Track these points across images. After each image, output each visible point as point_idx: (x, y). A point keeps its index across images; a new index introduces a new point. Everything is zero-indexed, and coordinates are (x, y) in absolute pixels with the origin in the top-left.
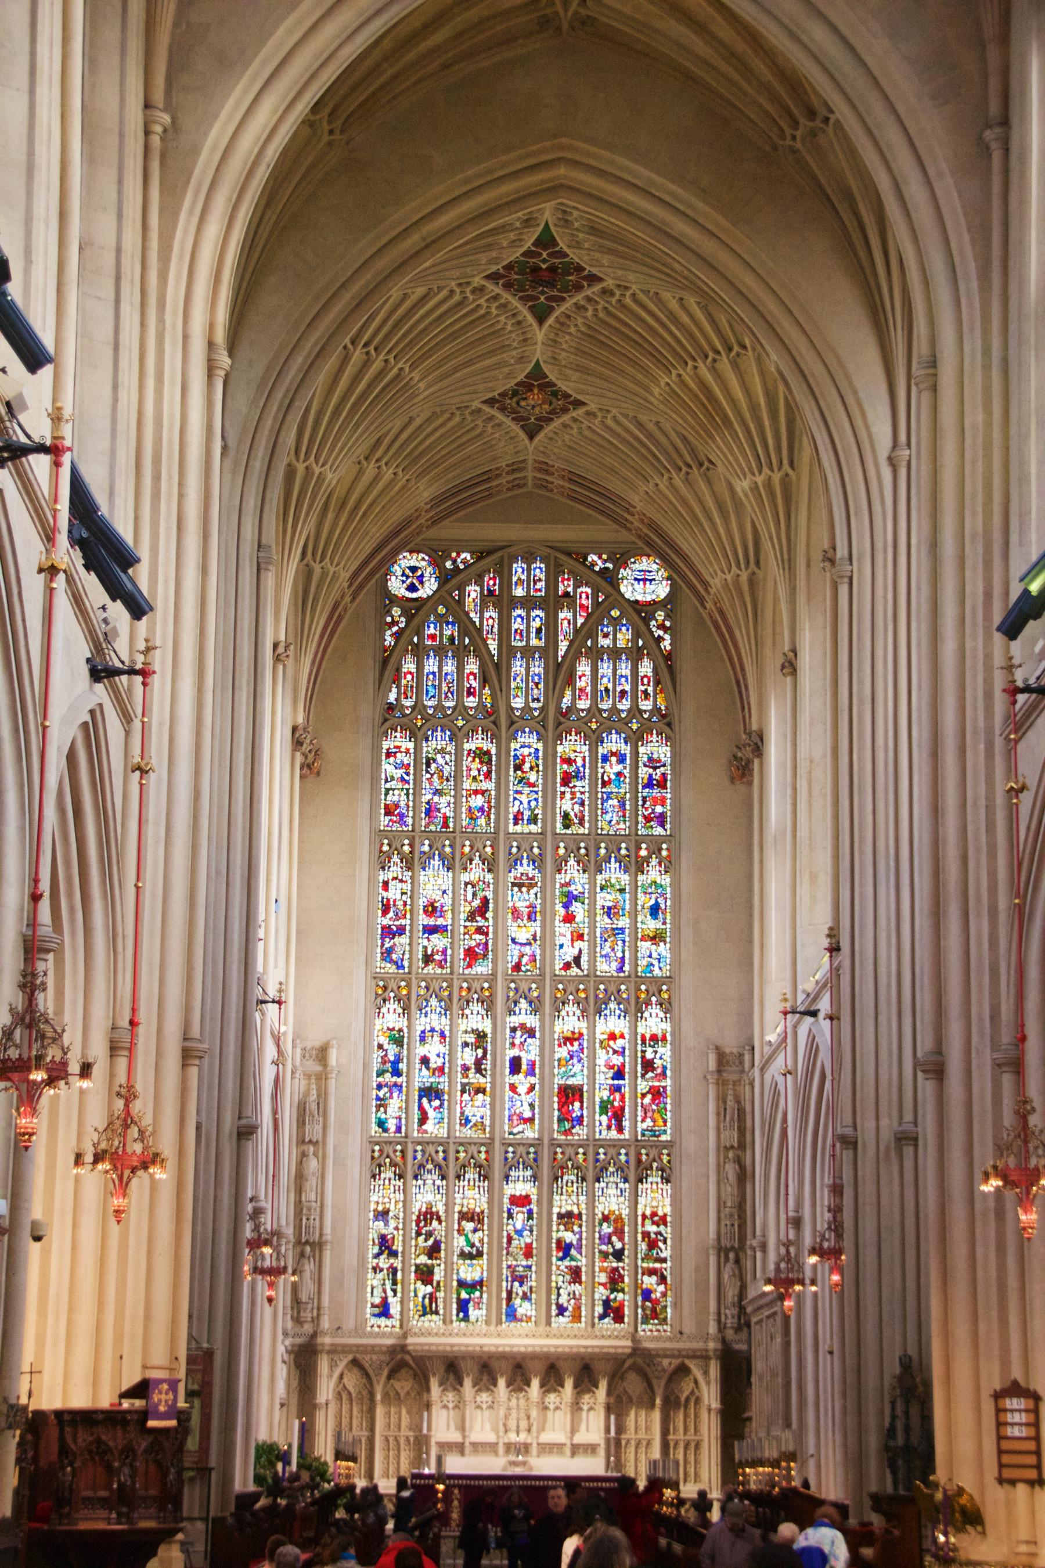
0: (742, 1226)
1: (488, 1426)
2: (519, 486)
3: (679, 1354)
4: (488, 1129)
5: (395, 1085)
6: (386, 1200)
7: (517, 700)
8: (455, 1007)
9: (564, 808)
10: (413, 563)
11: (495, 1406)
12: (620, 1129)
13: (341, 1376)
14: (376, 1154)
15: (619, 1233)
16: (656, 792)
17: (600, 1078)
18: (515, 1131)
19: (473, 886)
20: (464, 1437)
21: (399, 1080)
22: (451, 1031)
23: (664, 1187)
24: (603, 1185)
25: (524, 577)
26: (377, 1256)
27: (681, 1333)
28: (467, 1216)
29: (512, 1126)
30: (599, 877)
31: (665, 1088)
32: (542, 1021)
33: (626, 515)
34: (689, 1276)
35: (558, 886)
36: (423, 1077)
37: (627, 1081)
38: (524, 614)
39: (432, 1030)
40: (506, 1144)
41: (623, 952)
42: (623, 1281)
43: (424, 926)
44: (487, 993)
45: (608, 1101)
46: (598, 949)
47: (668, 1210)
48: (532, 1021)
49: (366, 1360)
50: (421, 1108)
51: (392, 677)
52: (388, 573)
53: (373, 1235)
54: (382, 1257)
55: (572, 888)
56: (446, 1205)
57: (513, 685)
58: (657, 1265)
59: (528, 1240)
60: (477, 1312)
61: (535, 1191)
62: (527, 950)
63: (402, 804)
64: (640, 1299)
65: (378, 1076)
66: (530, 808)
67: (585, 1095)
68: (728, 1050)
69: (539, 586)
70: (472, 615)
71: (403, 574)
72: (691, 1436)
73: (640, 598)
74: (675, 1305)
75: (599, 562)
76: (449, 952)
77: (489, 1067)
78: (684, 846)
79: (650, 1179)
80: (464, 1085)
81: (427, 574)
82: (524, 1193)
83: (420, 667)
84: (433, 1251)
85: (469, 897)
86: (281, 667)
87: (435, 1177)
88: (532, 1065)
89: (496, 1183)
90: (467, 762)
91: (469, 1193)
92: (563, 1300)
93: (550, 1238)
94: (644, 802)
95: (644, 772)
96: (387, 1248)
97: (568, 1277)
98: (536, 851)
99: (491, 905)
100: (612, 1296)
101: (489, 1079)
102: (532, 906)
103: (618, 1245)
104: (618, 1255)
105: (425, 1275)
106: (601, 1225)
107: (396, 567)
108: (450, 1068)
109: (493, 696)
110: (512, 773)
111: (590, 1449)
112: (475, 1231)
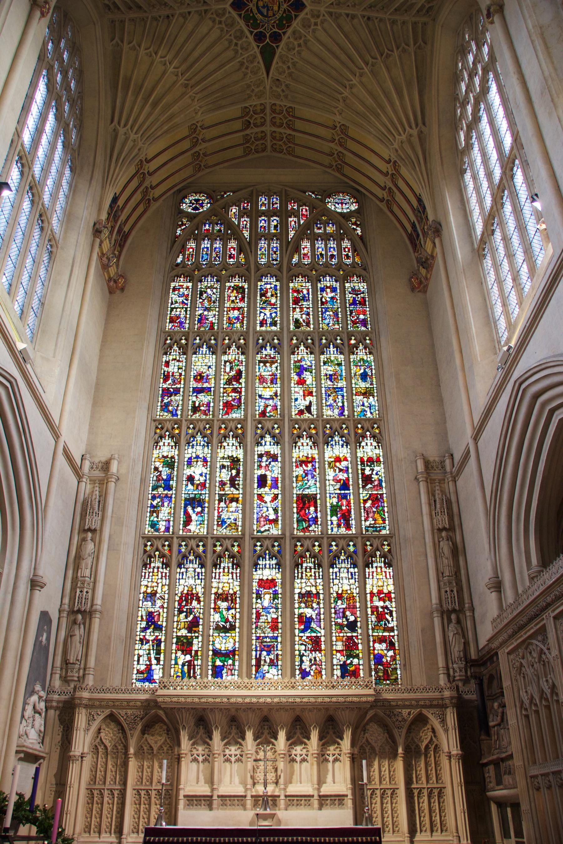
0: (460, 590)
1: (237, 780)
4: (240, 528)
6: (155, 584)
8: (215, 441)
9: (295, 316)
11: (244, 759)
12: (348, 527)
13: (99, 731)
14: (148, 548)
15: (352, 608)
16: (359, 308)
18: (262, 529)
19: (231, 363)
20: (213, 790)
21: (171, 492)
22: (211, 457)
23: (387, 570)
24: (336, 570)
26: (144, 630)
28: (222, 597)
30: (322, 357)
31: (382, 495)
32: (283, 449)
34: (415, 637)
35: (292, 362)
37: (351, 491)
39: (197, 457)
41: (343, 403)
42: (357, 649)
44: (240, 431)
45: (337, 506)
46: (324, 401)
47: (391, 588)
48: (275, 450)
49: (121, 713)
50: (186, 513)
53: (142, 612)
54: (148, 631)
55: (303, 363)
57: (259, 253)
58: (386, 634)
59: (275, 616)
61: (279, 576)
62: (271, 402)
63: (182, 316)
64: (373, 663)
65: (152, 491)
66: (271, 317)
67: (319, 501)
68: (431, 459)
69: (275, 206)
70: (234, 220)
72: (433, 784)
74: (404, 667)
76: (212, 404)
77: (241, 483)
79: (375, 565)
80: (221, 496)
82: (270, 578)
84: (193, 626)
85: (228, 369)
87: (196, 566)
88: (275, 480)
89: (247, 568)
91: (224, 579)
92: (306, 665)
93: (293, 614)
95: (349, 297)
96: (154, 623)
97: (310, 646)
99: (243, 375)
100: (349, 662)
101: (241, 491)
103: (352, 618)
108: (210, 484)
110: (258, 298)
111: (338, 799)
112: (229, 609)
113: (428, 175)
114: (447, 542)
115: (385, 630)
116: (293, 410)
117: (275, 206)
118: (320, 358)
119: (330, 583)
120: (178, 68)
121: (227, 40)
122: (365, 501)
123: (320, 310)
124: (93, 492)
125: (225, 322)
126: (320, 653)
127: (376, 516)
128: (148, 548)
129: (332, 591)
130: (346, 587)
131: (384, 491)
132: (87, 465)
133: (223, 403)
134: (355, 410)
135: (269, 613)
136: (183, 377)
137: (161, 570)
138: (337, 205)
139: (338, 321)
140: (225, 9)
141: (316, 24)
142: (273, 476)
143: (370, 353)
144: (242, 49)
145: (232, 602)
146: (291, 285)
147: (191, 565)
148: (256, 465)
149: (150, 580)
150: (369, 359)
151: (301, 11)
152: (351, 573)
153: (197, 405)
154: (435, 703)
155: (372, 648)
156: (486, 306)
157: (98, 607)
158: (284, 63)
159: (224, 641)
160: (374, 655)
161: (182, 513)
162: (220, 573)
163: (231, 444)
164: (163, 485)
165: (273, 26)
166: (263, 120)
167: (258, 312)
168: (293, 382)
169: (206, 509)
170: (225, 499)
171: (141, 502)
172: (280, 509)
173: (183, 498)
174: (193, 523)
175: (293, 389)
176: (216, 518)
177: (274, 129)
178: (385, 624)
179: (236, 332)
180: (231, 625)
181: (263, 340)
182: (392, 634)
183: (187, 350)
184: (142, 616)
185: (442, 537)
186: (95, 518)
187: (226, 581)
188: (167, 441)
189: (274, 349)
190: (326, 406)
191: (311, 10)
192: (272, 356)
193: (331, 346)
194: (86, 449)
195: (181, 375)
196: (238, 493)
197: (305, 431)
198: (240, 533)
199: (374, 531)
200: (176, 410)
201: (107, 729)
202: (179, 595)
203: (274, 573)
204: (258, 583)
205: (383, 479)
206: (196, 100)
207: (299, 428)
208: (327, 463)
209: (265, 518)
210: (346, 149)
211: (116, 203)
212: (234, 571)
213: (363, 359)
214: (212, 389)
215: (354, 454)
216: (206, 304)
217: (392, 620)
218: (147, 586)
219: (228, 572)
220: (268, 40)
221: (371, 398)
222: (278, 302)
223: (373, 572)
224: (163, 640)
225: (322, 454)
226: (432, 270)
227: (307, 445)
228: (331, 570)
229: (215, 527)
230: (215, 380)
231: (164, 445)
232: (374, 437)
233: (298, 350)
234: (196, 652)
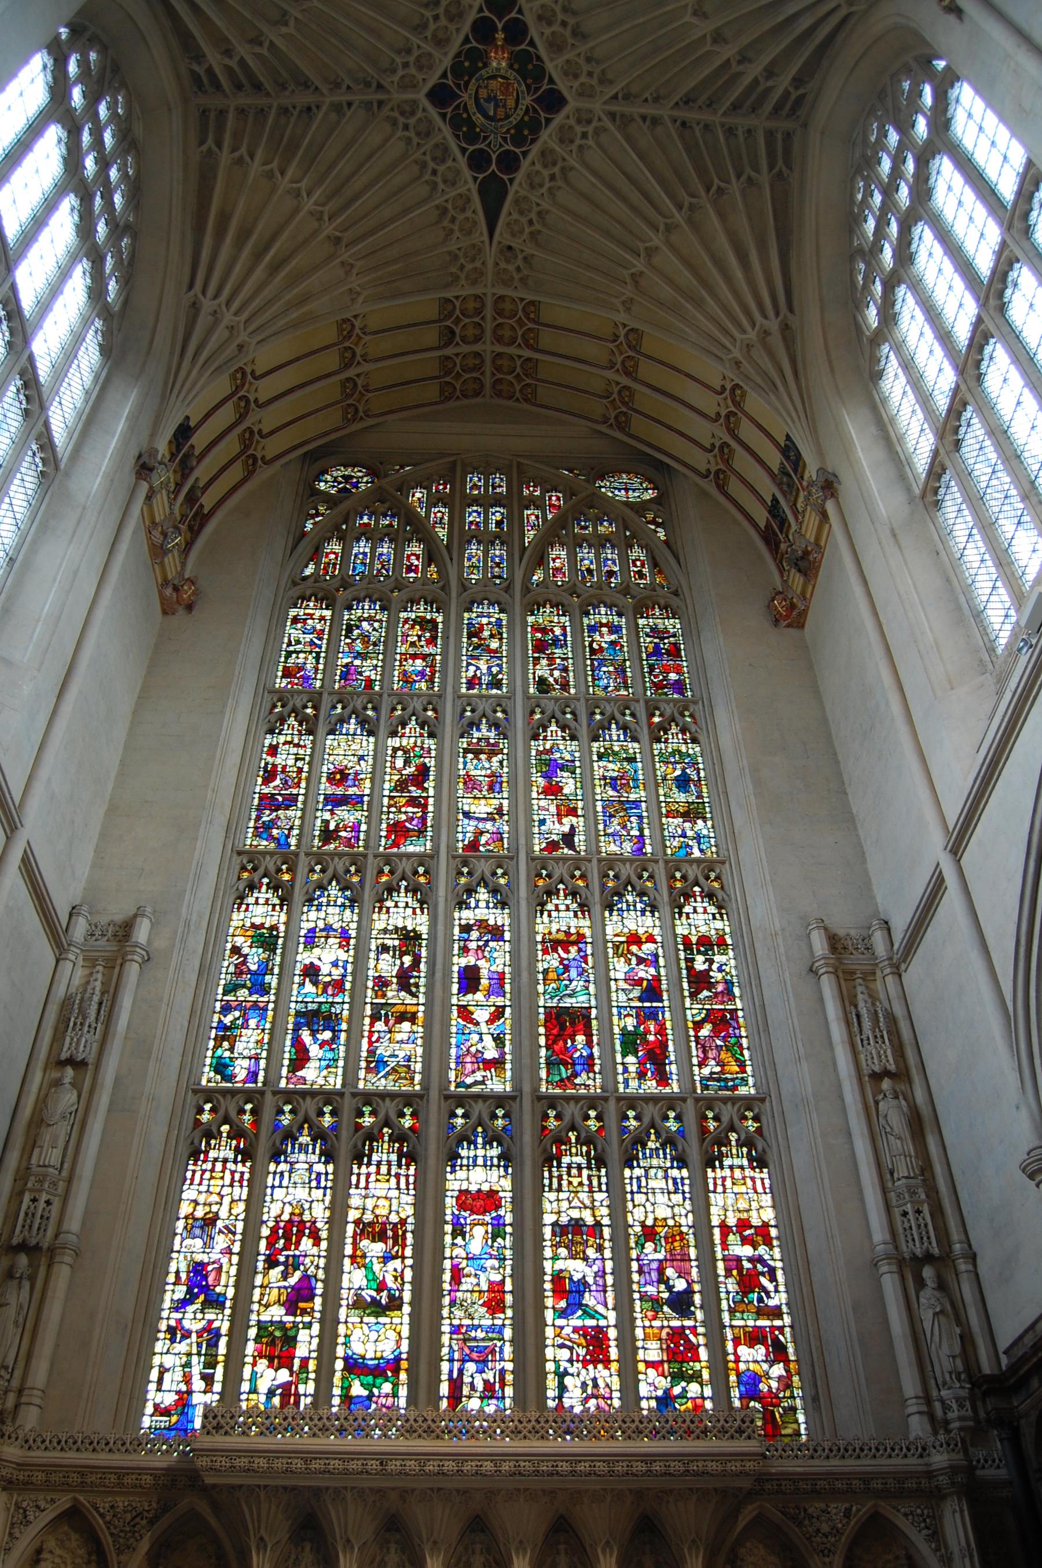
4: (418, 1078)
6: (215, 1198)
8: (368, 895)
9: (539, 673)
12: (663, 1079)
18: (469, 1080)
19: (405, 752)
22: (358, 929)
23: (757, 1175)
26: (181, 1305)
28: (374, 1230)
30: (595, 745)
32: (514, 917)
35: (534, 753)
37: (666, 1003)
39: (328, 928)
41: (641, 830)
45: (635, 1033)
46: (601, 827)
51: (310, 551)
54: (191, 1308)
56: (332, 1208)
57: (466, 564)
59: (498, 1278)
61: (507, 1183)
62: (489, 826)
63: (308, 666)
65: (224, 995)
67: (594, 1023)
68: (841, 933)
74: (813, 1403)
76: (364, 827)
79: (727, 1162)
82: (485, 1187)
83: (346, 552)
85: (399, 763)
87: (314, 1158)
89: (432, 1161)
91: (379, 1188)
96: (206, 1289)
97: (582, 1352)
100: (677, 1390)
101: (422, 1000)
103: (680, 1285)
104: (681, 1303)
112: (386, 1259)
114: (895, 1102)
115: (763, 1312)
116: (536, 841)
117: (498, 490)
118: (590, 747)
119: (625, 1201)
120: (323, 205)
121: (416, 162)
122: (698, 1025)
123: (588, 662)
124: (88, 983)
126: (606, 1367)
127: (723, 1055)
128: (205, 1117)
130: (663, 1212)
132: (80, 928)
134: (668, 843)
135: (483, 1269)
136: (304, 775)
137: (230, 1166)
139: (625, 682)
140: (415, 102)
141: (584, 135)
142: (493, 968)
143: (694, 741)
144: (445, 182)
146: (531, 619)
147: (302, 1157)
148: (456, 946)
149: (203, 1188)
150: (691, 752)
151: (558, 111)
152: (674, 1180)
153: (332, 827)
154: (911, 1484)
155: (731, 1357)
156: (952, 591)
158: (521, 213)
161: (288, 1043)
162: (368, 1175)
164: (248, 983)
165: (505, 139)
166: (477, 332)
167: (464, 664)
168: (535, 789)
169: (343, 1036)
170: (386, 1015)
171: (198, 1013)
172: (508, 1037)
173: (293, 1012)
174: (312, 1064)
175: (535, 802)
176: (364, 1054)
177: (499, 349)
178: (760, 1300)
179: (419, 696)
180: (391, 1297)
181: (473, 711)
182: (778, 1323)
183: (316, 724)
184: (177, 1273)
185: (881, 1091)
187: (383, 1193)
188: (263, 894)
191: (578, 110)
193: (614, 726)
195: (300, 770)
197: (561, 882)
198: (417, 1088)
200: (288, 836)
201: (58, 1552)
202: (271, 1224)
203: (495, 1178)
204: (458, 1198)
206: (355, 271)
207: (549, 876)
208: (610, 945)
209: (474, 1056)
210: (635, 380)
211: (188, 438)
212: (402, 1172)
213: (679, 751)
214: (366, 799)
216: (359, 646)
217: (776, 1291)
218: (196, 1203)
219: (389, 1173)
220: (494, 166)
221: (700, 822)
223: (724, 1179)
224: (224, 1330)
226: (816, 576)
227: (568, 909)
228: (627, 1172)
229: (362, 1074)
230: (372, 780)
232: (710, 896)
233: (545, 731)
234: (305, 1361)
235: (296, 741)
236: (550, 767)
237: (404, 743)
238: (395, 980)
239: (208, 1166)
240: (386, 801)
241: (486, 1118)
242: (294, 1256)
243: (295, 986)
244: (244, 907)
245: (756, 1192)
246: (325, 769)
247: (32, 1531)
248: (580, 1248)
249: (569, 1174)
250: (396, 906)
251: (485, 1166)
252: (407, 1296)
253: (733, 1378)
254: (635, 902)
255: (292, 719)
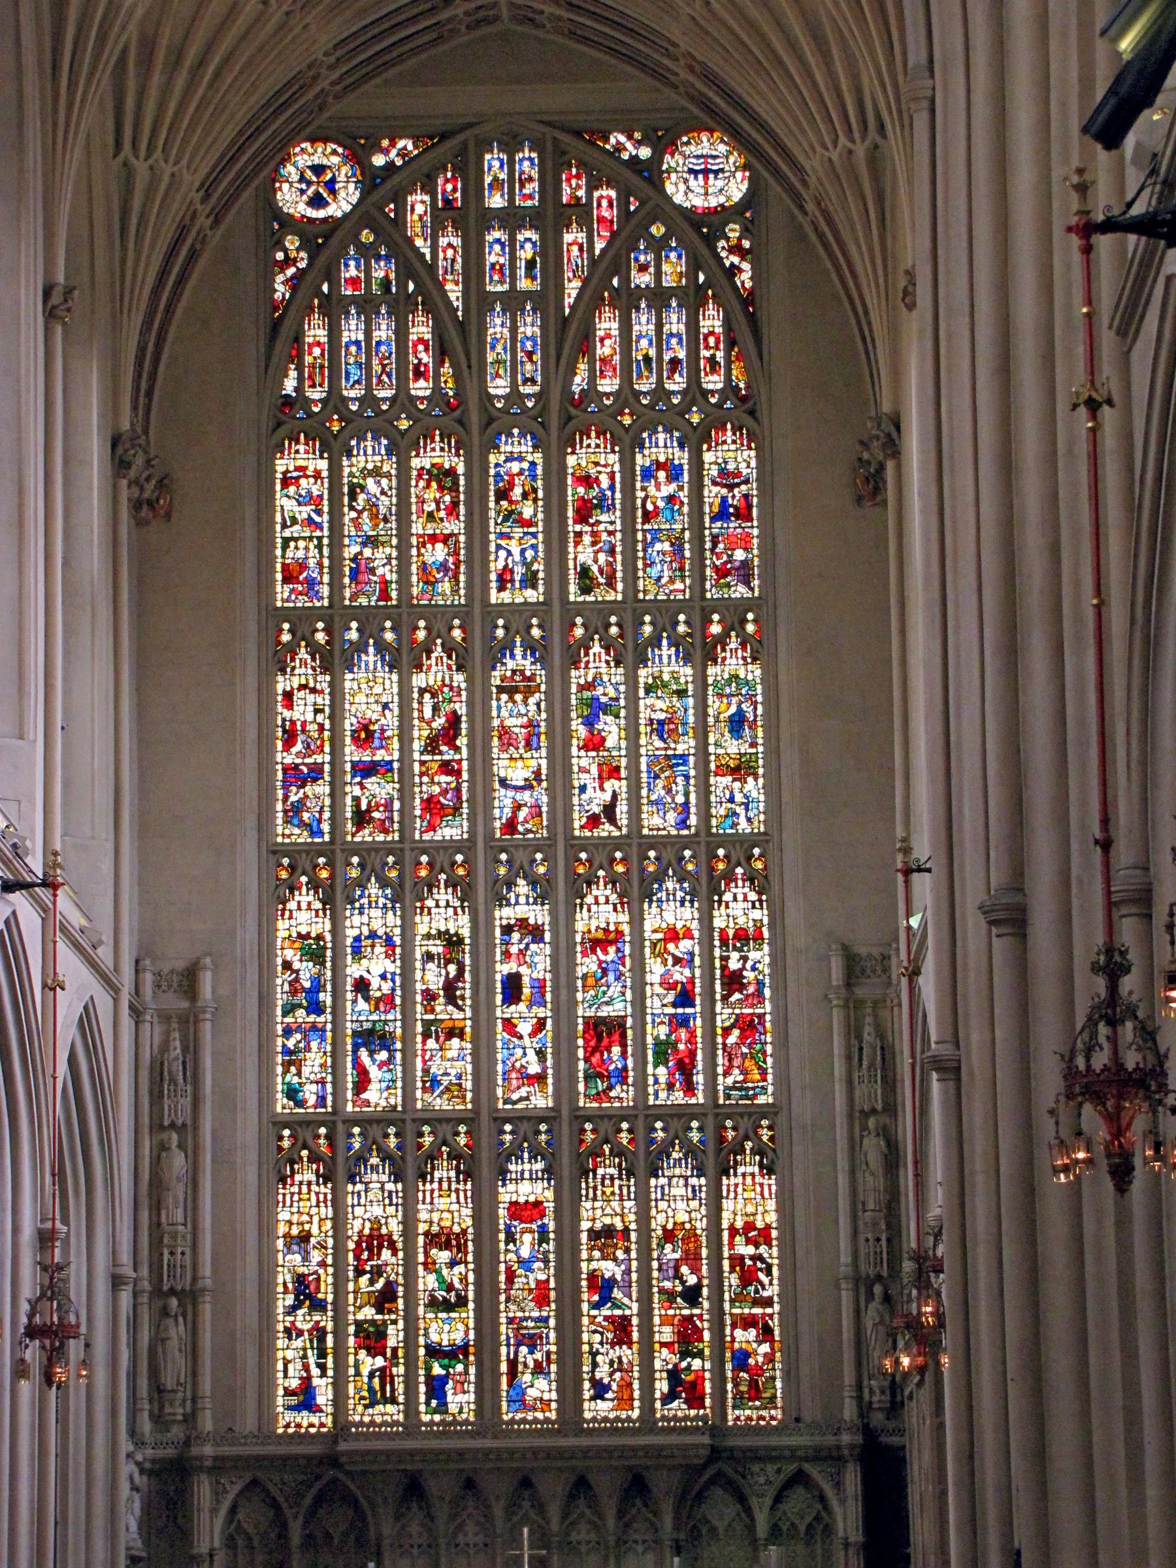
2: (488, 21)
3: (793, 1454)
4: (469, 1095)
5: (314, 1027)
6: (305, 1218)
7: (499, 382)
9: (581, 558)
10: (317, 160)
12: (689, 1089)
13: (233, 1510)
15: (694, 1259)
17: (654, 1005)
18: (515, 1096)
19: (434, 696)
21: (321, 1019)
22: (403, 935)
24: (663, 1181)
25: (503, 176)
26: (292, 1310)
27: (797, 1420)
28: (440, 1239)
29: (507, 1089)
30: (642, 672)
31: (761, 1017)
33: (666, 61)
35: (574, 689)
36: (359, 1011)
37: (698, 1009)
38: (504, 237)
39: (373, 935)
40: (500, 1120)
41: (687, 794)
42: (701, 1340)
43: (354, 765)
45: (667, 1043)
46: (644, 792)
47: (772, 1218)
48: (538, 915)
52: (275, 177)
53: (283, 1277)
54: (300, 1312)
55: (599, 691)
56: (404, 1223)
57: (490, 357)
58: (758, 1311)
59: (542, 1277)
60: (460, 1398)
61: (550, 1194)
62: (526, 796)
63: (312, 563)
65: (285, 1015)
67: (629, 1033)
68: (863, 951)
70: (419, 242)
71: (302, 179)
73: (698, 202)
75: (629, 145)
76: (397, 805)
78: (782, 613)
79: (741, 1170)
80: (427, 1024)
81: (342, 178)
82: (532, 1199)
83: (334, 333)
85: (428, 713)
86: (59, 329)
87: (385, 1178)
88: (540, 985)
90: (416, 489)
91: (442, 1203)
92: (602, 1373)
93: (577, 1271)
94: (715, 543)
95: (712, 494)
96: (309, 1297)
97: (610, 1336)
98: (536, 632)
99: (464, 726)
100: (684, 1365)
101: (469, 1014)
102: (531, 724)
103: (692, 1280)
105: (372, 1340)
106: (661, 1247)
107: (290, 168)
108: (403, 997)
109: (457, 377)
110: (492, 505)
112: (452, 1264)
113: (884, 260)
116: (576, 815)
119: (650, 1208)
125: (414, 579)
127: (747, 1063)
128: (286, 1144)
129: (653, 1225)
130: (682, 1217)
131: (768, 1007)
133: (422, 800)
134: (713, 811)
135: (531, 1270)
136: (326, 734)
137: (314, 1188)
138: (692, 183)
139: (682, 569)
142: (535, 975)
145: (459, 1251)
147: (375, 1177)
148: (498, 950)
149: (295, 1210)
150: (750, 677)
152: (693, 1187)
153: (364, 807)
155: (728, 1339)
157: (208, 1282)
159: (447, 1328)
160: (733, 1352)
161: (349, 1065)
162: (432, 1191)
163: (442, 903)
164: (305, 1003)
167: (493, 548)
168: (575, 742)
169: (398, 1055)
170: (437, 1032)
172: (549, 1050)
173: (349, 1032)
174: (374, 1086)
175: (574, 761)
176: (419, 1073)
178: (757, 1292)
180: (458, 1296)
183: (332, 664)
184: (285, 1284)
186: (182, 1101)
187: (446, 1207)
189: (533, 654)
190: (650, 803)
192: (528, 673)
193: (665, 642)
194: (140, 948)
195: (321, 728)
196: (462, 1016)
197: (601, 867)
199: (741, 1098)
200: (320, 821)
203: (539, 1191)
205: (767, 981)
208: (647, 943)
209: (519, 1071)
212: (461, 1187)
213: (737, 677)
214: (396, 765)
215: (706, 920)
216: (367, 527)
217: (771, 1284)
218: (290, 1223)
221: (750, 780)
222: (540, 516)
223: (736, 1185)
225: (637, 921)
227: (607, 902)
228: (653, 1182)
229: (419, 1094)
230: (401, 741)
231: (299, 908)
234: (395, 1350)
235: (312, 685)
236: (594, 710)
237: (431, 683)
238: (442, 993)
239: (295, 1189)
240: (416, 767)
241: (530, 1135)
242: (378, 1266)
243: (349, 1004)
244: (287, 914)
245: (763, 1197)
246: (347, 726)
247: (230, 1497)
248: (611, 1250)
249: (603, 1185)
250: (437, 906)
251: (531, 1179)
252: (471, 1296)
253: (728, 1355)
254: (675, 890)
255: (303, 650)
